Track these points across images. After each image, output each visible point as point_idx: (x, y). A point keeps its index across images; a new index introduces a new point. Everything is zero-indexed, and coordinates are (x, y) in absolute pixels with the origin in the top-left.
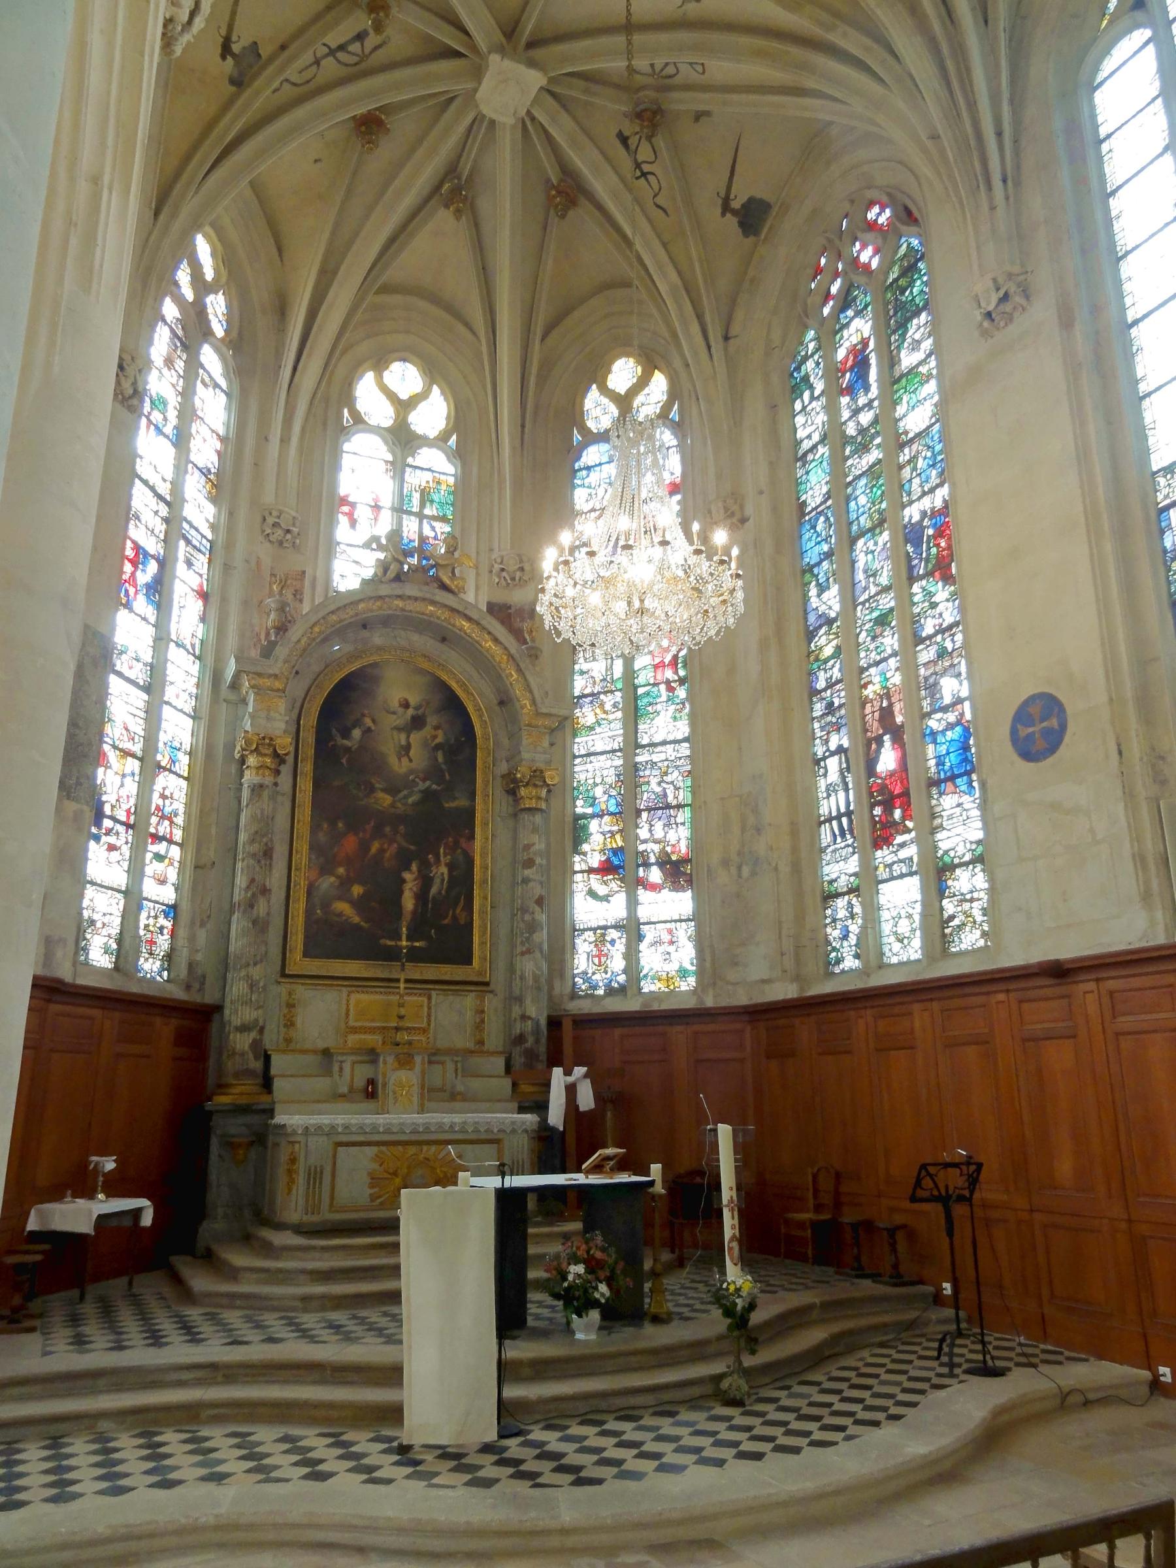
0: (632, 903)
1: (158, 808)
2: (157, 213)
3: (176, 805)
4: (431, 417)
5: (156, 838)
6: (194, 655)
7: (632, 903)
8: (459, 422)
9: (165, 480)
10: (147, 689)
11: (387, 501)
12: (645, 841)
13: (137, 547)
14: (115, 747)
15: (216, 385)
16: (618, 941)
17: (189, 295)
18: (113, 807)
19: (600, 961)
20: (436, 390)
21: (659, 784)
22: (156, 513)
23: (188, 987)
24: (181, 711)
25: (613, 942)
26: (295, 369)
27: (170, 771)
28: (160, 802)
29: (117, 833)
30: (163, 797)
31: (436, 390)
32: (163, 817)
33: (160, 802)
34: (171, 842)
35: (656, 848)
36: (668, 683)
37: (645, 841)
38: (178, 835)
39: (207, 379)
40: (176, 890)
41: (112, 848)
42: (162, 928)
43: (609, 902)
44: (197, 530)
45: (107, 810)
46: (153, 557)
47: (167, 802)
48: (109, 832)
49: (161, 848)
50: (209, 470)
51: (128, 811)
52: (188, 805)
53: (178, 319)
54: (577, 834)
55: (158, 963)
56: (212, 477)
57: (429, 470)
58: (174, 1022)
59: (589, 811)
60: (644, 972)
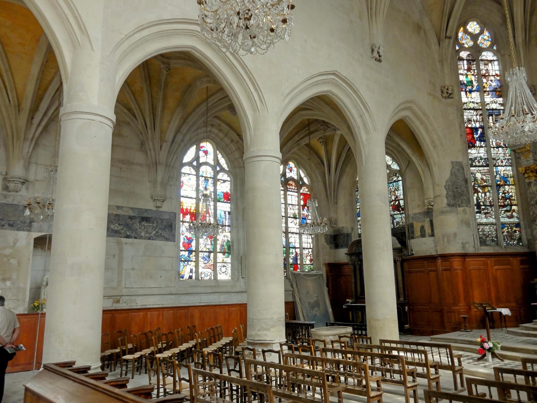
1: (502, 197)
2: (439, 45)
3: (511, 194)
5: (504, 206)
6: (506, 147)
9: (477, 103)
10: (487, 166)
13: (471, 128)
14: (479, 186)
15: (491, 61)
17: (471, 43)
18: (483, 202)
22: (477, 115)
23: (529, 248)
24: (505, 166)
26: (514, 37)
27: (505, 185)
28: (503, 195)
29: (487, 209)
30: (504, 193)
32: (506, 199)
33: (503, 195)
34: (511, 205)
39: (486, 62)
40: (518, 219)
42: (515, 231)
44: (496, 109)
45: (481, 203)
46: (479, 128)
47: (507, 194)
48: (484, 209)
49: (508, 208)
50: (496, 88)
51: (490, 202)
52: (516, 193)
53: (469, 55)
55: (516, 241)
56: (499, 90)
58: (519, 258)
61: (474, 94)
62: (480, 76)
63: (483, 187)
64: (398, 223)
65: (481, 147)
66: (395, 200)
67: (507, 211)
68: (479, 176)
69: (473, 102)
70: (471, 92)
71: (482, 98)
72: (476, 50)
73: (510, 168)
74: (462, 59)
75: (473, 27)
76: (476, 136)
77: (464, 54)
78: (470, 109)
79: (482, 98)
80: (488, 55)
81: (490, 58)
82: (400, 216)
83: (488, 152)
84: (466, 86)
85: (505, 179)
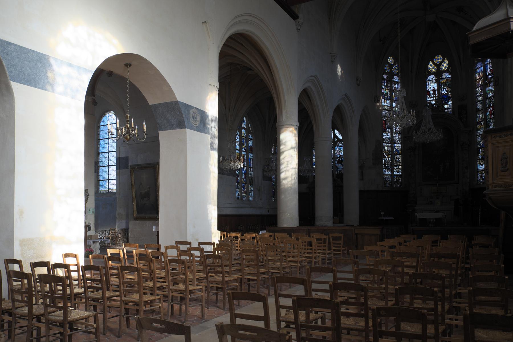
4: (444, 66)
5: (396, 166)
8: (450, 65)
11: (436, 88)
15: (397, 83)
20: (445, 59)
31: (445, 59)
34: (399, 165)
36: (492, 118)
38: (401, 164)
41: (388, 169)
54: (479, 152)
57: (446, 78)
61: (388, 101)
62: (391, 91)
63: (388, 155)
64: (340, 171)
65: (389, 132)
66: (340, 158)
67: (397, 168)
68: (386, 148)
69: (387, 106)
70: (387, 99)
71: (392, 104)
72: (391, 75)
73: (400, 145)
74: (384, 79)
75: (390, 60)
76: (387, 126)
77: (385, 76)
78: (386, 110)
79: (392, 104)
80: (396, 79)
81: (397, 80)
82: (342, 167)
83: (392, 135)
84: (385, 96)
85: (397, 151)
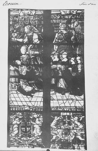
0: (47, 100)
7: (47, 100)
12: (56, 63)
16: (37, 119)
19: (26, 129)
21: (65, 29)
25: (34, 119)
35: (62, 67)
37: (56, 63)
43: (32, 96)
59: (21, 40)
60: (54, 138)
